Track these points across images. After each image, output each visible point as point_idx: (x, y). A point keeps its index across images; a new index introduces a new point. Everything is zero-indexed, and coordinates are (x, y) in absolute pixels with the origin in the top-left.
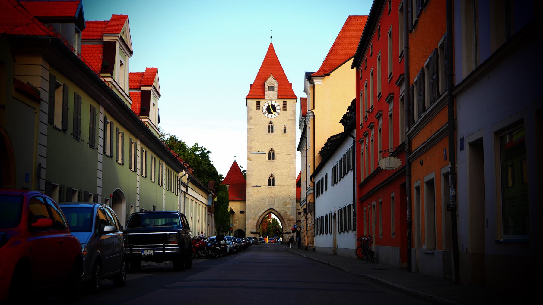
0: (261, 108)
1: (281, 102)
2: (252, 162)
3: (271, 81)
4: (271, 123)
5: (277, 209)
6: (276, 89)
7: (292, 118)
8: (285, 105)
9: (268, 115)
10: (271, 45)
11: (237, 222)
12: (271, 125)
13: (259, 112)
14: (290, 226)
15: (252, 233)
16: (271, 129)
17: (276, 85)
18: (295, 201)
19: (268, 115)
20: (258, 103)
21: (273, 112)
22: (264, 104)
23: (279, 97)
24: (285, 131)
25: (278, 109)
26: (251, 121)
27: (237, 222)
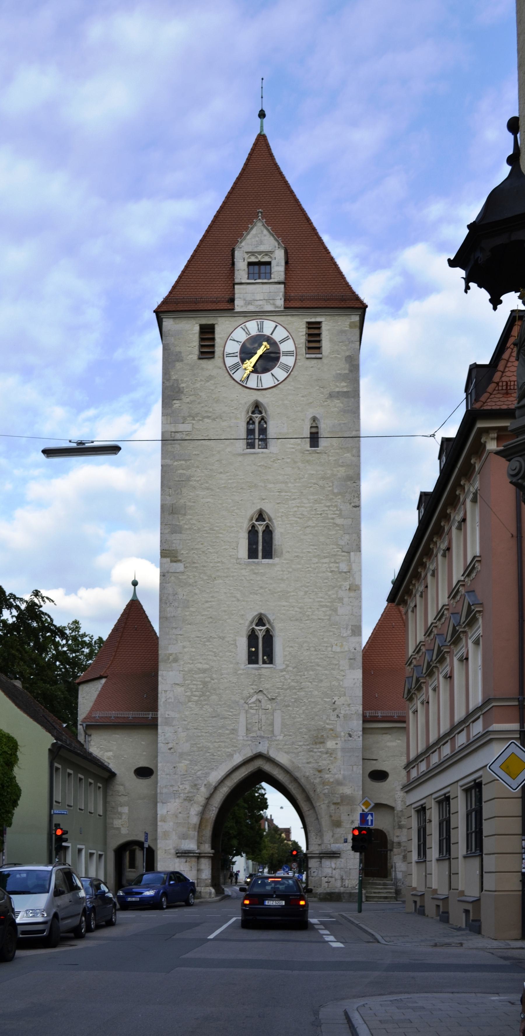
0: (218, 350)
1: (299, 323)
2: (180, 567)
3: (259, 240)
4: (257, 407)
5: (282, 758)
7: (343, 386)
11: (125, 810)
12: (257, 417)
14: (337, 824)
15: (182, 854)
16: (257, 433)
18: (357, 724)
20: (207, 333)
22: (233, 336)
23: (292, 305)
24: (314, 439)
26: (177, 404)
27: (125, 810)
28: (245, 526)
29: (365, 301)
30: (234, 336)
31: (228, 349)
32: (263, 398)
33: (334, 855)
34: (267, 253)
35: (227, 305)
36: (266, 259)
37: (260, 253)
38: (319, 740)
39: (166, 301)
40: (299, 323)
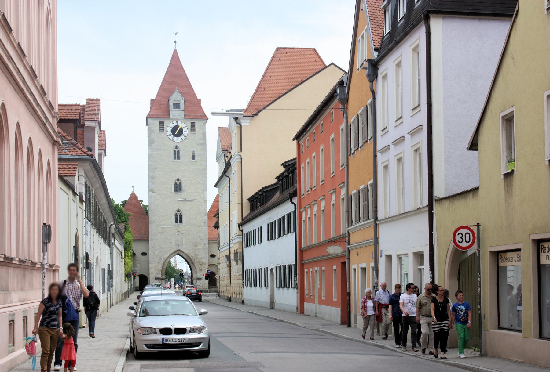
2: (155, 194)
3: (176, 97)
4: (177, 147)
5: (185, 251)
7: (202, 142)
9: (173, 138)
10: (175, 51)
12: (177, 150)
13: (163, 135)
16: (177, 155)
17: (182, 102)
18: (207, 241)
19: (173, 138)
22: (169, 126)
23: (186, 117)
25: (186, 132)
28: (174, 183)
30: (170, 125)
32: (178, 145)
33: (200, 279)
35: (167, 116)
38: (196, 246)
39: (149, 115)
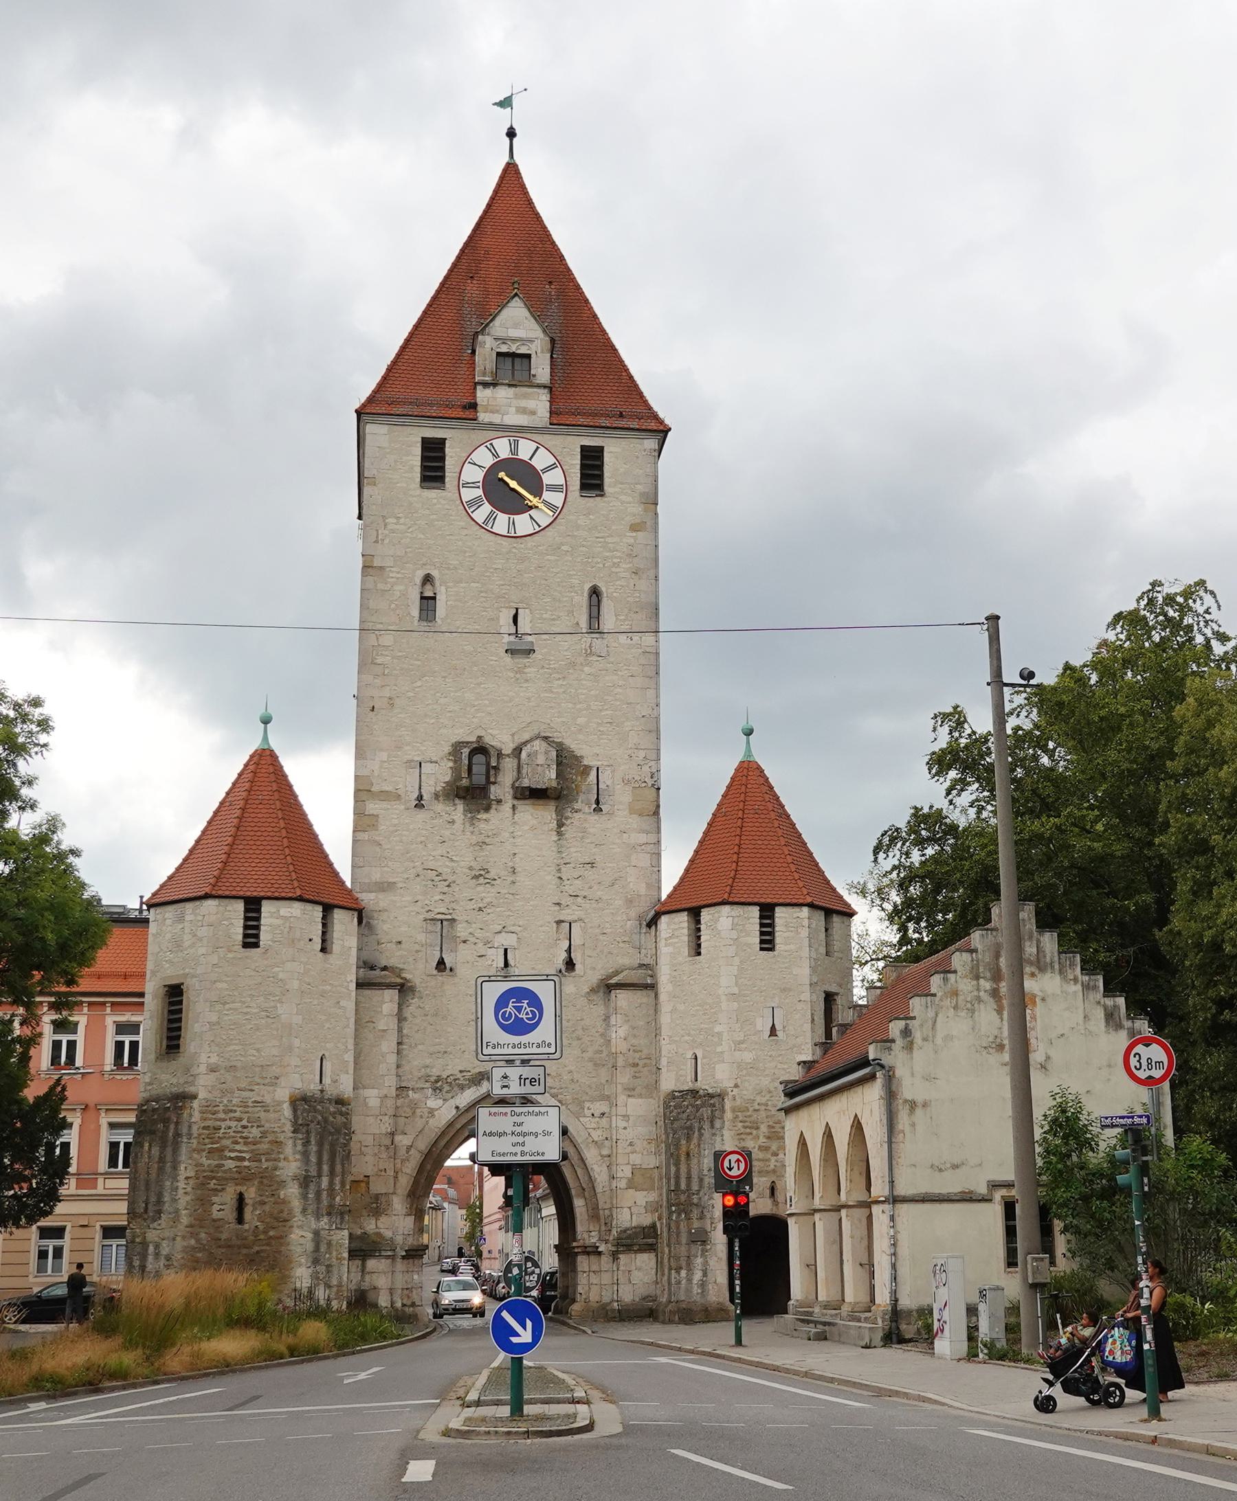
6: (542, 369)
8: (592, 462)
9: (491, 518)
10: (511, 173)
19: (491, 518)
20: (433, 453)
21: (532, 499)
23: (560, 418)
25: (554, 488)
29: (667, 422)
31: (465, 477)
34: (524, 341)
36: (523, 350)
37: (514, 340)
40: (571, 446)
